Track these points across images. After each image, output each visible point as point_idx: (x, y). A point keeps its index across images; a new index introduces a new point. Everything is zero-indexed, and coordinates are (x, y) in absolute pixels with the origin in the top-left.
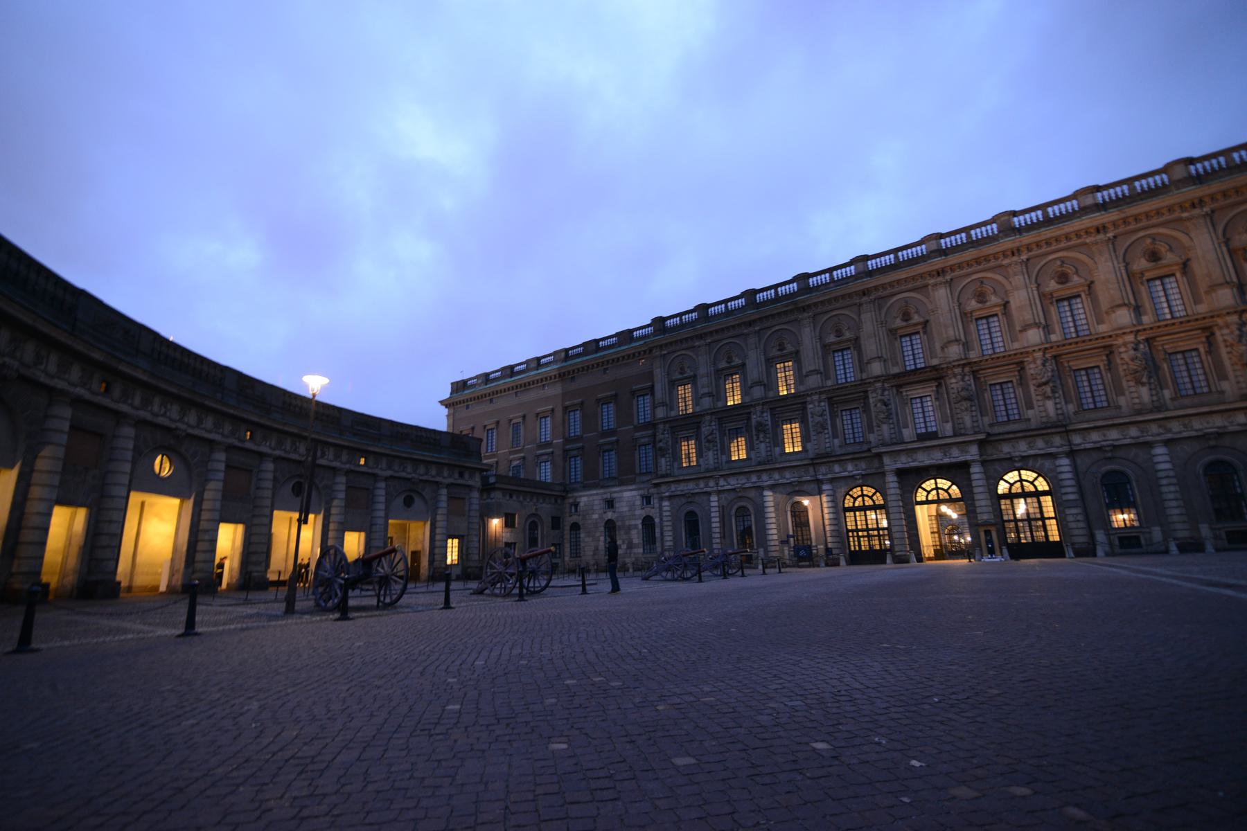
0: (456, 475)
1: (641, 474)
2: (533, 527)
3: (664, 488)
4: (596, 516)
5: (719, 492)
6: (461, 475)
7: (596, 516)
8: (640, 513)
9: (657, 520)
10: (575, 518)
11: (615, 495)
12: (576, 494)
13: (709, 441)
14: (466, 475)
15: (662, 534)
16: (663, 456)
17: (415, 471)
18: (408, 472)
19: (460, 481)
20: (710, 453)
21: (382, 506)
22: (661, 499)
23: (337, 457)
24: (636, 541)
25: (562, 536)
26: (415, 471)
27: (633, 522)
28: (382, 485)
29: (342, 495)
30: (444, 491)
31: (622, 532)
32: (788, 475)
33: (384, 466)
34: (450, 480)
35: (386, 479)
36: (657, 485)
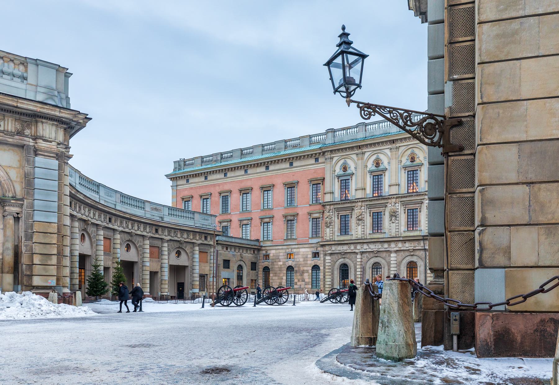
0: (203, 239)
1: (312, 238)
2: (240, 268)
3: (327, 248)
4: (281, 263)
5: (362, 253)
6: (206, 238)
7: (281, 263)
8: (311, 262)
9: (322, 268)
10: (266, 264)
11: (295, 250)
12: (267, 248)
13: (359, 220)
14: (209, 239)
15: (324, 277)
16: (328, 227)
17: (182, 237)
18: (178, 237)
19: (206, 242)
20: (360, 227)
21: (166, 257)
22: (325, 255)
23: (145, 229)
24: (307, 280)
25: (257, 275)
26: (182, 237)
27: (305, 268)
28: (166, 245)
29: (148, 251)
30: (197, 248)
31: (298, 274)
32: (407, 245)
33: (166, 234)
34: (200, 242)
35: (168, 241)
36: (323, 246)
